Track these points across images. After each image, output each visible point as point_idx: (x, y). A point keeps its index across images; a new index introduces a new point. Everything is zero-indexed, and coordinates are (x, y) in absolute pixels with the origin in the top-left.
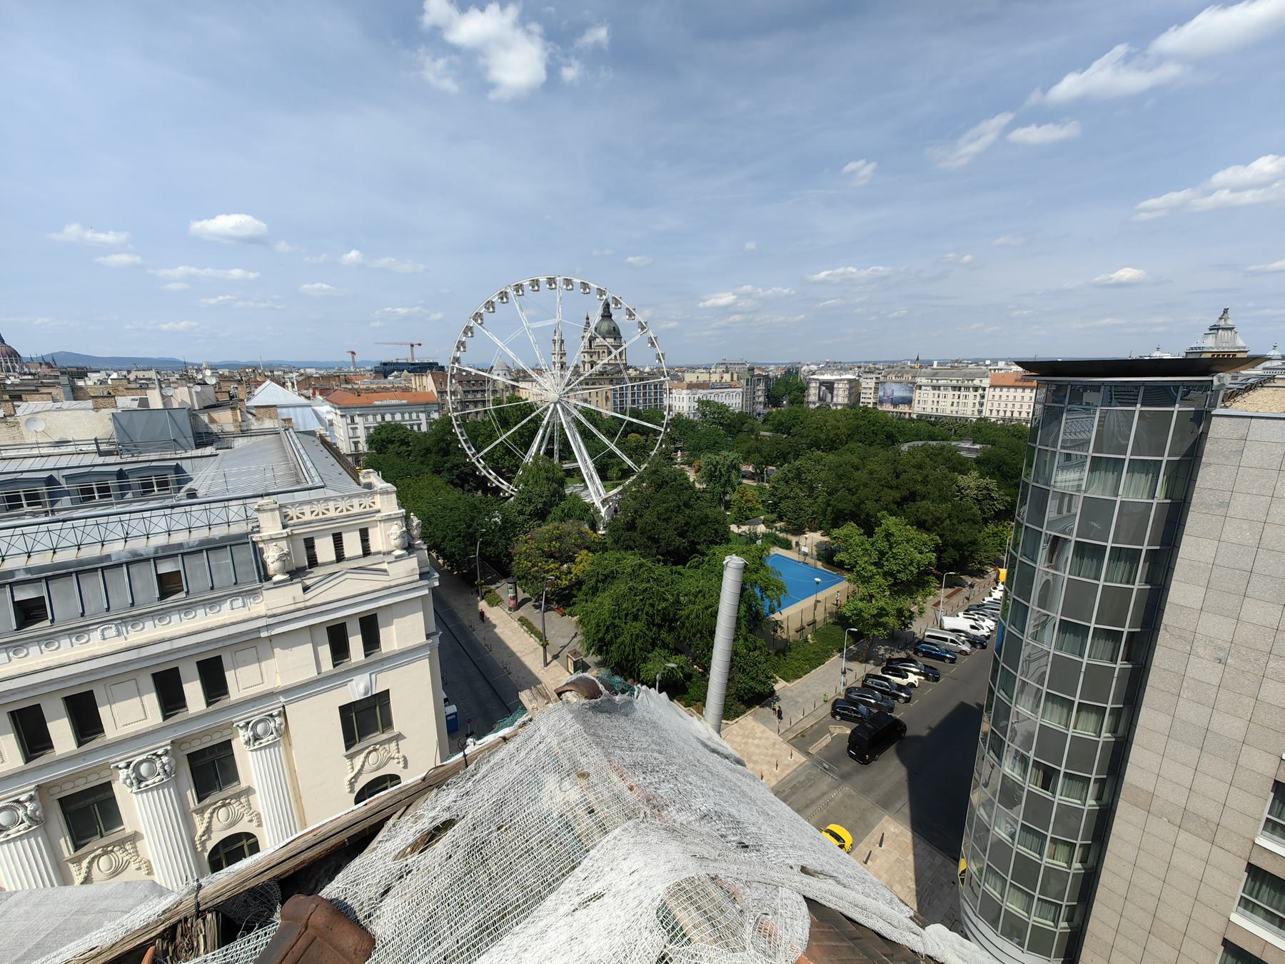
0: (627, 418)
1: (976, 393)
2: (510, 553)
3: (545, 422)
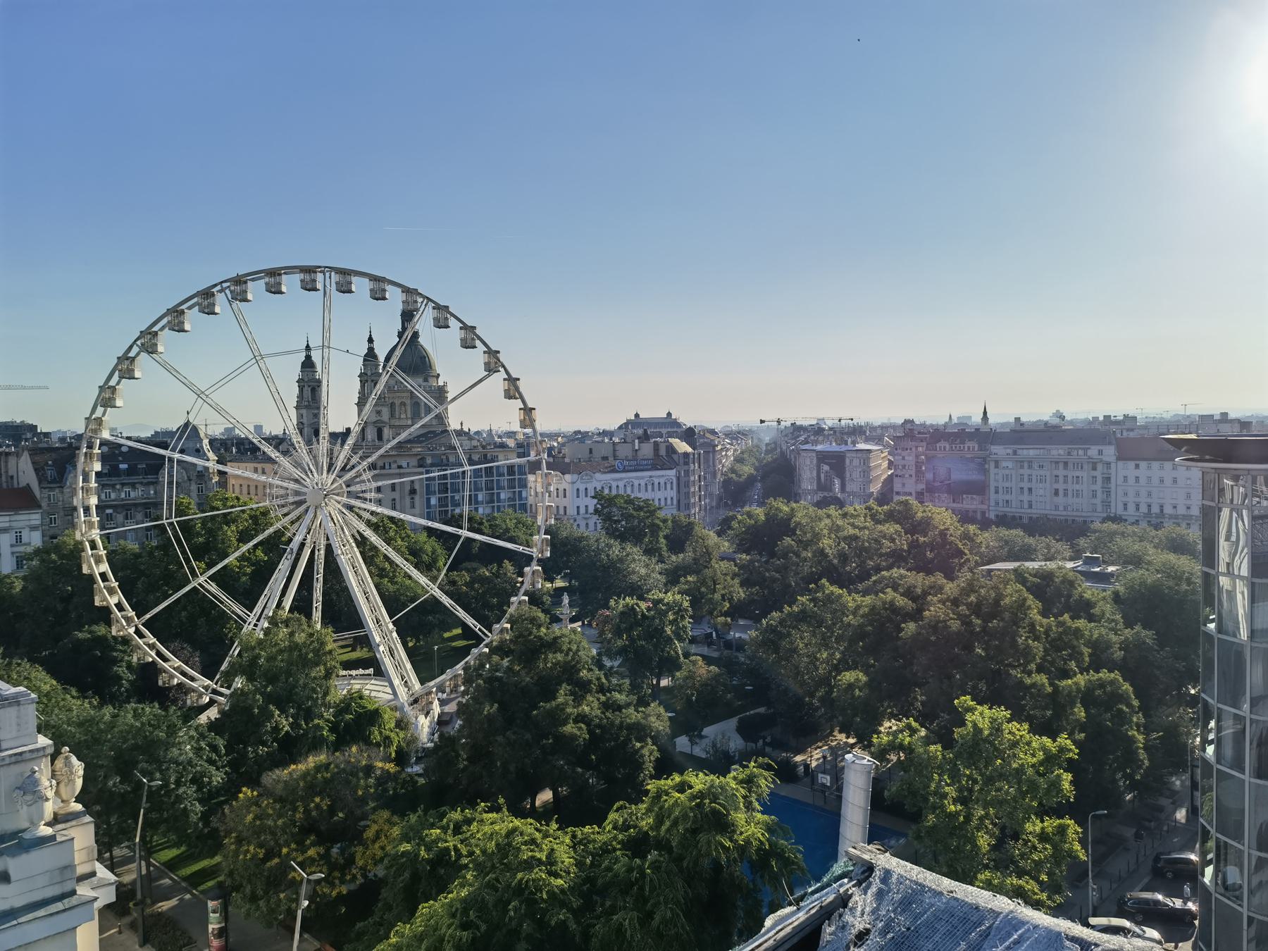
0: (465, 533)
1: (1094, 473)
2: (216, 830)
3: (295, 545)
